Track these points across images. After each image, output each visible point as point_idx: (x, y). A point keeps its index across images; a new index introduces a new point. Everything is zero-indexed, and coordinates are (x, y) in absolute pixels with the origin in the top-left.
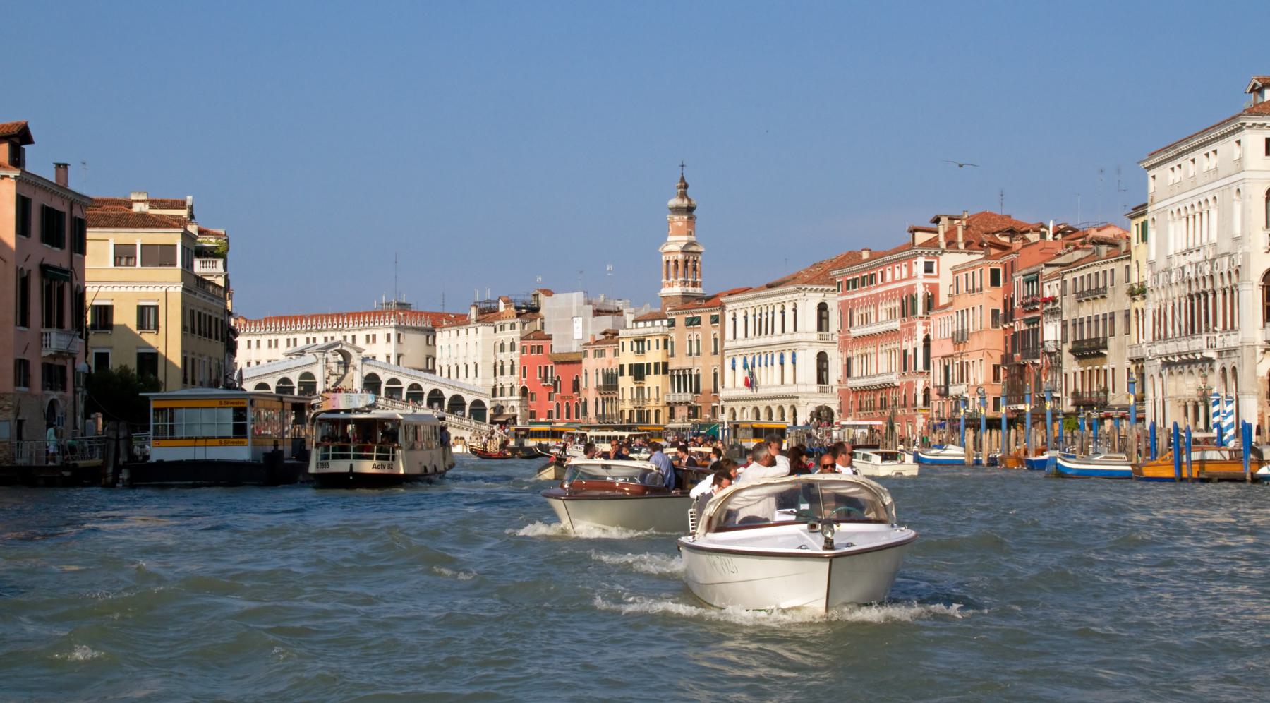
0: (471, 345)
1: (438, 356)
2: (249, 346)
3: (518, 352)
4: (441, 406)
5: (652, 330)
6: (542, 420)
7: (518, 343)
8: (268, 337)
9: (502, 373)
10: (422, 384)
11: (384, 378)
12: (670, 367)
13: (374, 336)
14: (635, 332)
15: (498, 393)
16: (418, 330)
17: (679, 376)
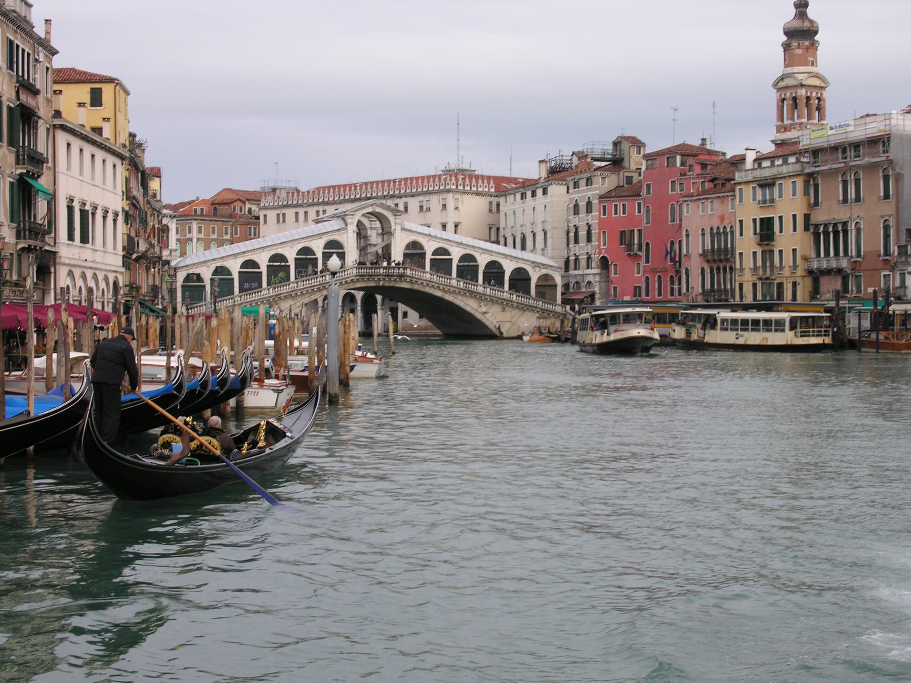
0: (540, 208)
1: (502, 226)
2: (297, 220)
4: (501, 283)
5: (785, 169)
6: (627, 298)
7: (595, 202)
8: (316, 208)
9: (576, 241)
10: (477, 255)
11: (429, 248)
12: (814, 219)
14: (759, 174)
15: (572, 265)
16: (478, 194)
17: (827, 234)
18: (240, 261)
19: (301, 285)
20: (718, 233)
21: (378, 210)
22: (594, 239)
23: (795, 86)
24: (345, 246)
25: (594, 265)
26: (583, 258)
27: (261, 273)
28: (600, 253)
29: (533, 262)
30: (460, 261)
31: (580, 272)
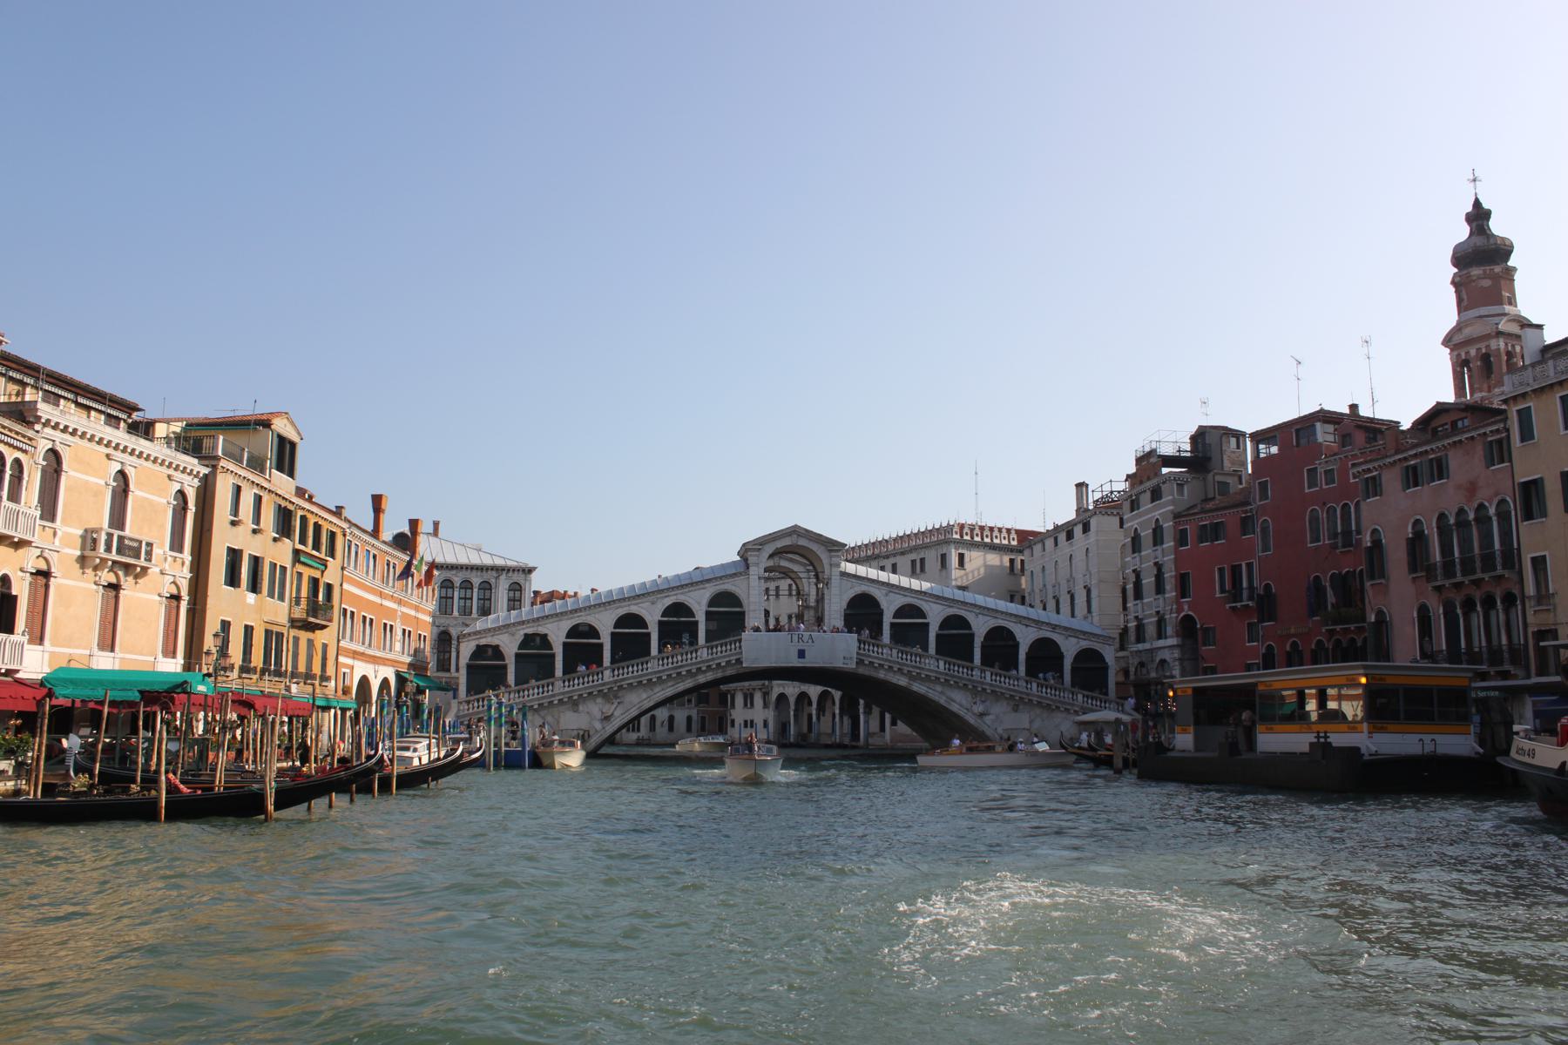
0: (1079, 557)
3: (1169, 544)
7: (1168, 525)
9: (1138, 595)
10: (970, 617)
13: (922, 560)
16: (993, 547)
18: (567, 625)
19: (669, 664)
20: (1462, 524)
21: (802, 542)
22: (1168, 587)
23: (1487, 337)
24: (745, 602)
25: (1170, 630)
26: (1150, 623)
27: (601, 646)
28: (1179, 610)
29: (1066, 629)
30: (942, 627)
31: (1147, 646)
